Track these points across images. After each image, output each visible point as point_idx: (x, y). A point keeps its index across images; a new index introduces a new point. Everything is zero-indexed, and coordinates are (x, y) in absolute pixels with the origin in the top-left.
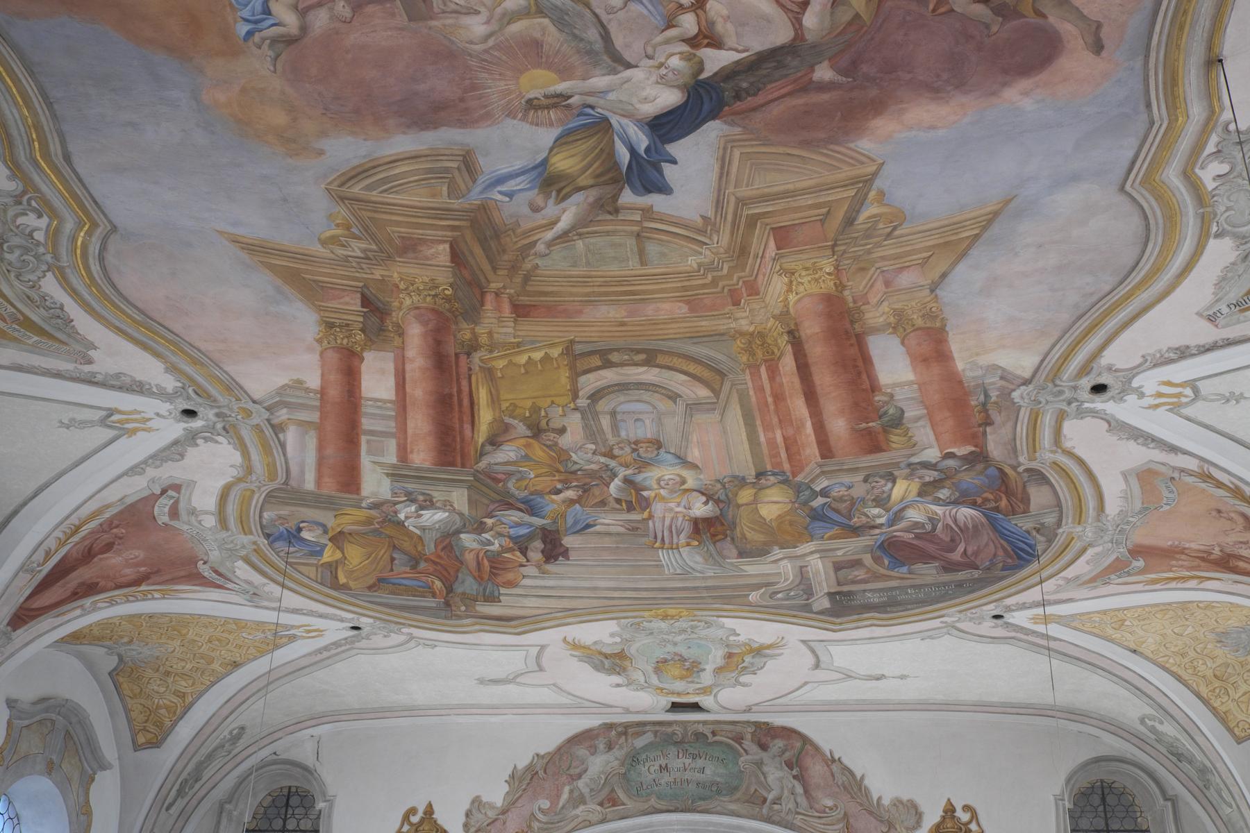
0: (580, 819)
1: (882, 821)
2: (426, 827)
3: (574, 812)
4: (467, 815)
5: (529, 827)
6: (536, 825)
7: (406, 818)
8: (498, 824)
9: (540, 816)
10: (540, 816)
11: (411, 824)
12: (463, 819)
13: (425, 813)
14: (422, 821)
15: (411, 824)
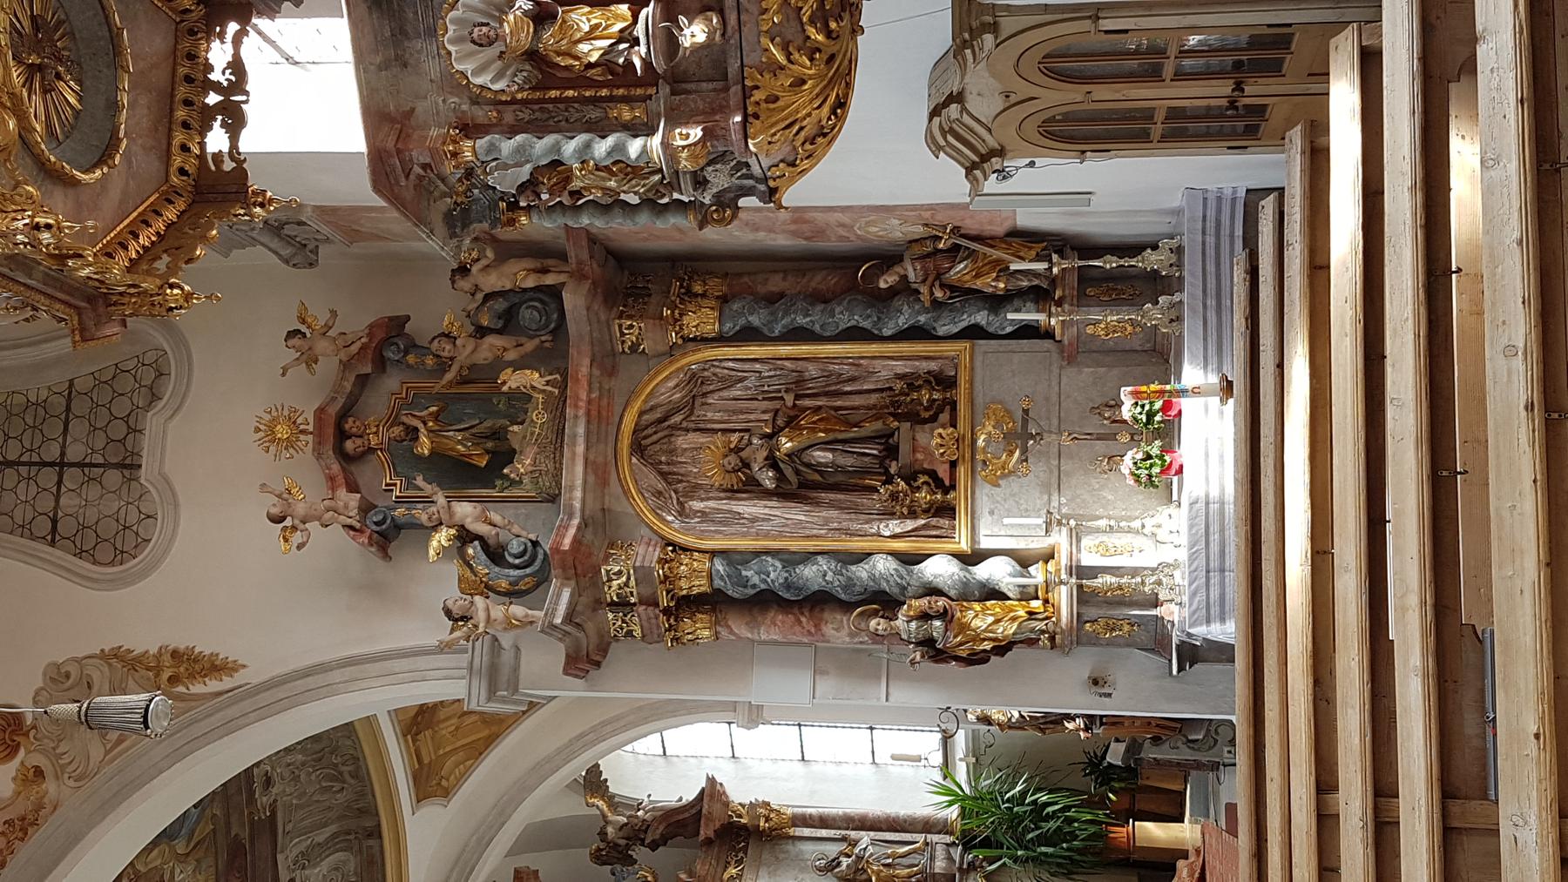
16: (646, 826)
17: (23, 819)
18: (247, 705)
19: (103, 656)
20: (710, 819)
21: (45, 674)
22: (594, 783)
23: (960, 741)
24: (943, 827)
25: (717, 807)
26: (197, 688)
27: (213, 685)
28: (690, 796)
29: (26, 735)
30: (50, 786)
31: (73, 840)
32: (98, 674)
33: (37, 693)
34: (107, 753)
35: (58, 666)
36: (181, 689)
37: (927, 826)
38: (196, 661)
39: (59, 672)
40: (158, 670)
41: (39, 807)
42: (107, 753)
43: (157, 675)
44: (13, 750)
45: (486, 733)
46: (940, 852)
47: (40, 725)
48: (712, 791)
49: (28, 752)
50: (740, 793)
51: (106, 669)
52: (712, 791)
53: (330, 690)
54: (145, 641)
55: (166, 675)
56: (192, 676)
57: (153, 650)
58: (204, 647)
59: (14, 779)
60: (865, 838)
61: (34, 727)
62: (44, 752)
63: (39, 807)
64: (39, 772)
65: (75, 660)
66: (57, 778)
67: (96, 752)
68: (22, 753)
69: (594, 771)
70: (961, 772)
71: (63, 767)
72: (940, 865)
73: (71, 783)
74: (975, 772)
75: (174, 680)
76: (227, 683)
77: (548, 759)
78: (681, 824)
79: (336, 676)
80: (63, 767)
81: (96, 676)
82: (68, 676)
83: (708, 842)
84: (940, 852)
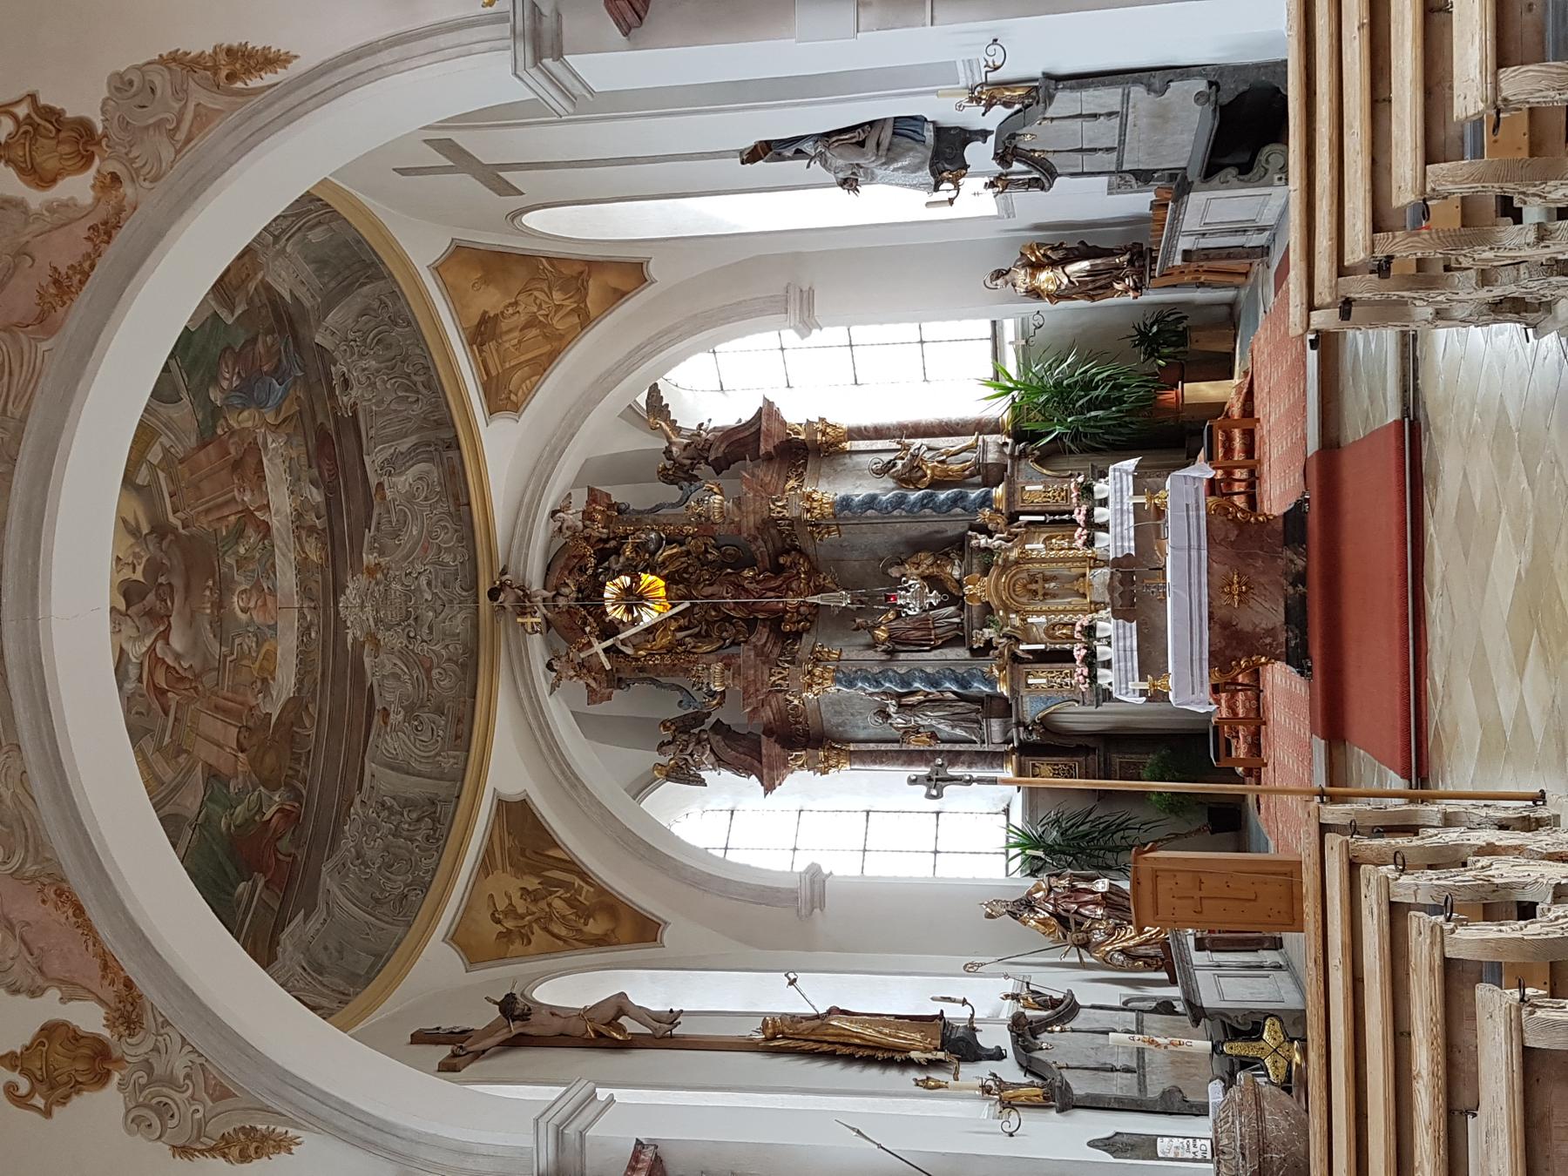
0: (19, 791)
1: (16, 267)
2: (36, 1064)
3: (8, 802)
4: (16, 992)
5: (33, 879)
6: (31, 869)
7: (21, 1101)
8: (28, 938)
9: (15, 862)
10: (15, 862)
11: (31, 1094)
12: (22, 999)
13: (14, 1068)
14: (24, 1072)
15: (31, 1094)
16: (708, 445)
17: (105, 223)
18: (303, 93)
19: (162, 61)
20: (769, 435)
21: (109, 84)
22: (657, 406)
23: (1009, 331)
24: (995, 428)
25: (775, 426)
26: (254, 83)
27: (269, 78)
28: (747, 415)
29: (99, 143)
30: (128, 190)
31: (154, 238)
32: (160, 79)
33: (104, 103)
34: (177, 152)
35: (120, 75)
36: (239, 85)
37: (981, 427)
38: (250, 56)
39: (123, 83)
40: (215, 69)
41: (119, 210)
42: (177, 152)
43: (215, 74)
44: (87, 160)
45: (547, 348)
46: (992, 449)
47: (111, 132)
48: (768, 411)
49: (103, 160)
50: (796, 413)
51: (166, 73)
52: (768, 411)
53: (380, 72)
54: (200, 42)
55: (224, 73)
56: (248, 72)
57: (209, 51)
58: (256, 43)
59: (93, 187)
60: (918, 442)
61: (105, 136)
62: (118, 159)
63: (119, 210)
64: (115, 178)
65: (138, 68)
66: (133, 180)
67: (167, 153)
68: (97, 161)
69: (654, 390)
70: (1011, 365)
71: (137, 170)
72: (992, 457)
73: (147, 184)
74: (1025, 365)
75: (231, 77)
76: (281, 75)
77: (610, 372)
78: (742, 443)
79: (384, 57)
80: (137, 170)
81: (158, 81)
82: (131, 83)
83: (769, 458)
84: (992, 449)
